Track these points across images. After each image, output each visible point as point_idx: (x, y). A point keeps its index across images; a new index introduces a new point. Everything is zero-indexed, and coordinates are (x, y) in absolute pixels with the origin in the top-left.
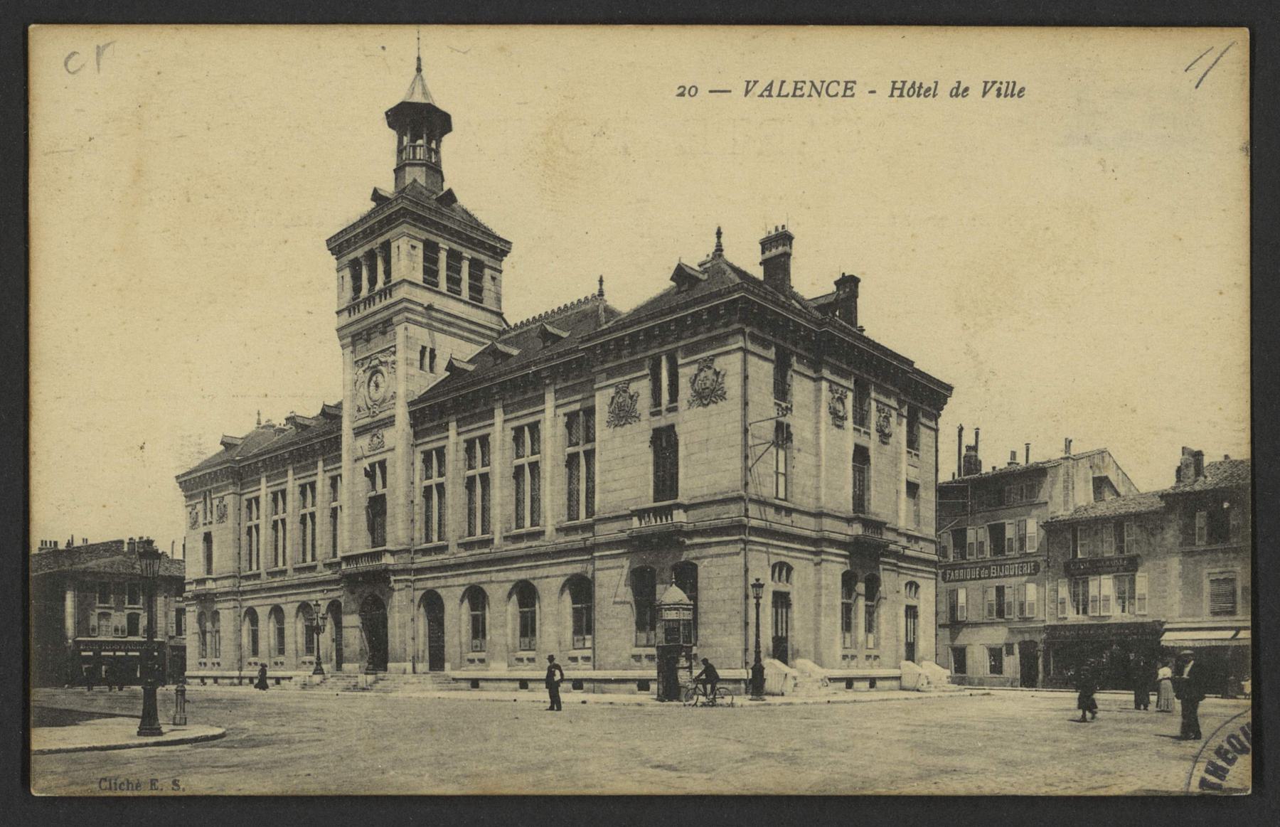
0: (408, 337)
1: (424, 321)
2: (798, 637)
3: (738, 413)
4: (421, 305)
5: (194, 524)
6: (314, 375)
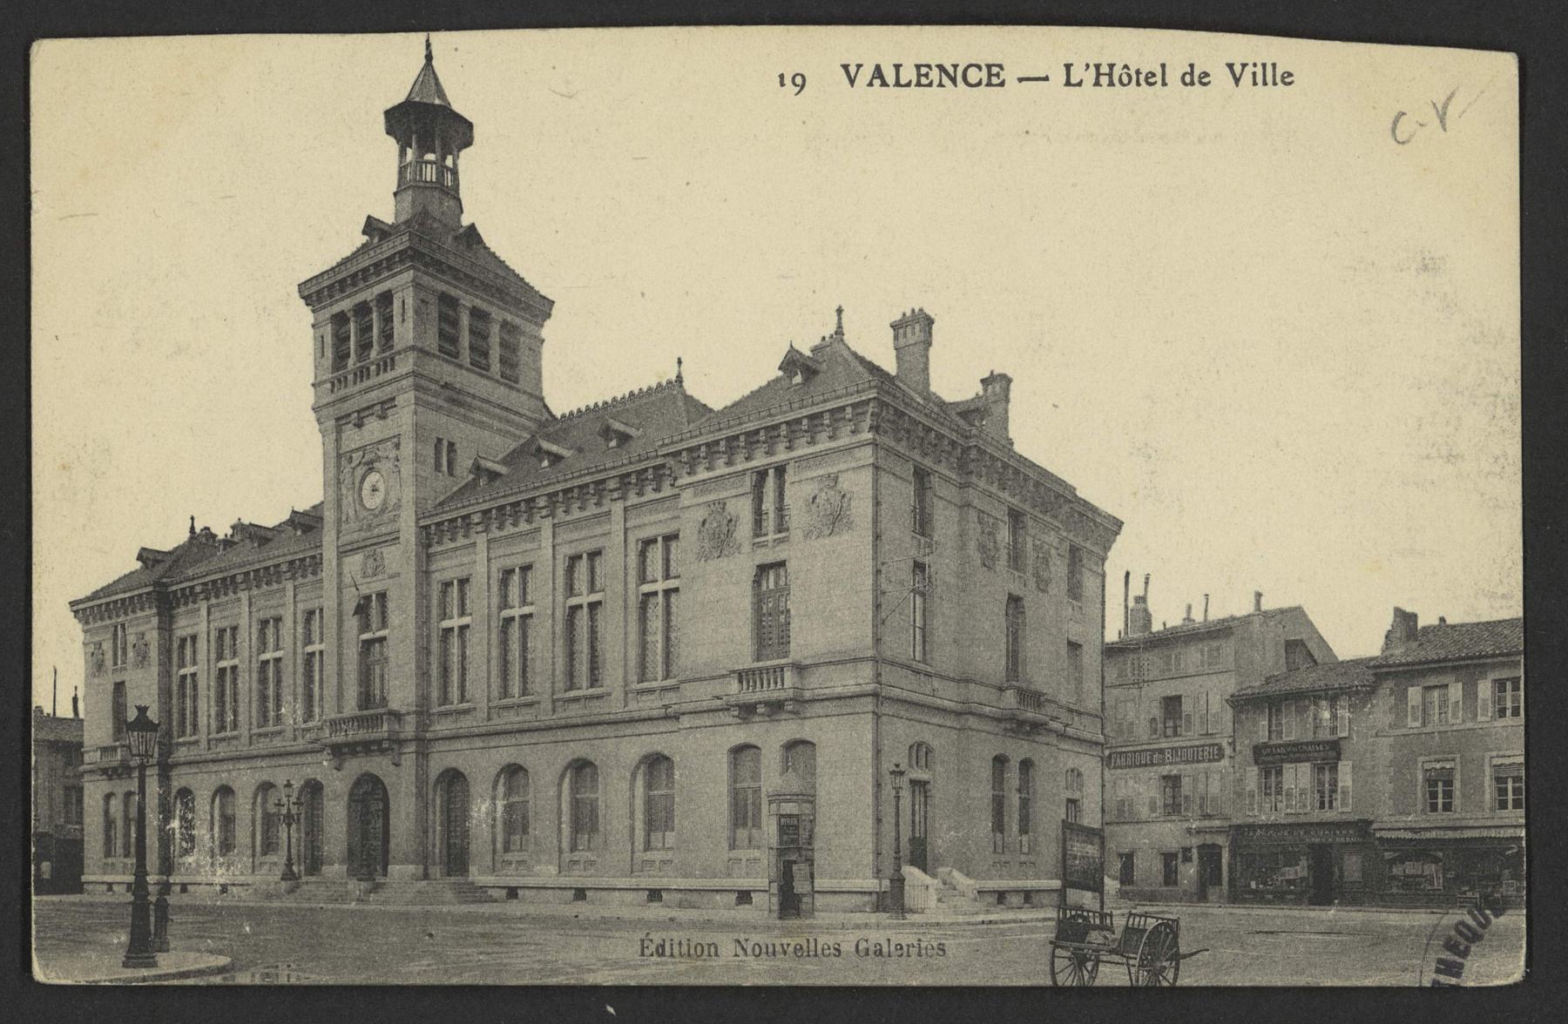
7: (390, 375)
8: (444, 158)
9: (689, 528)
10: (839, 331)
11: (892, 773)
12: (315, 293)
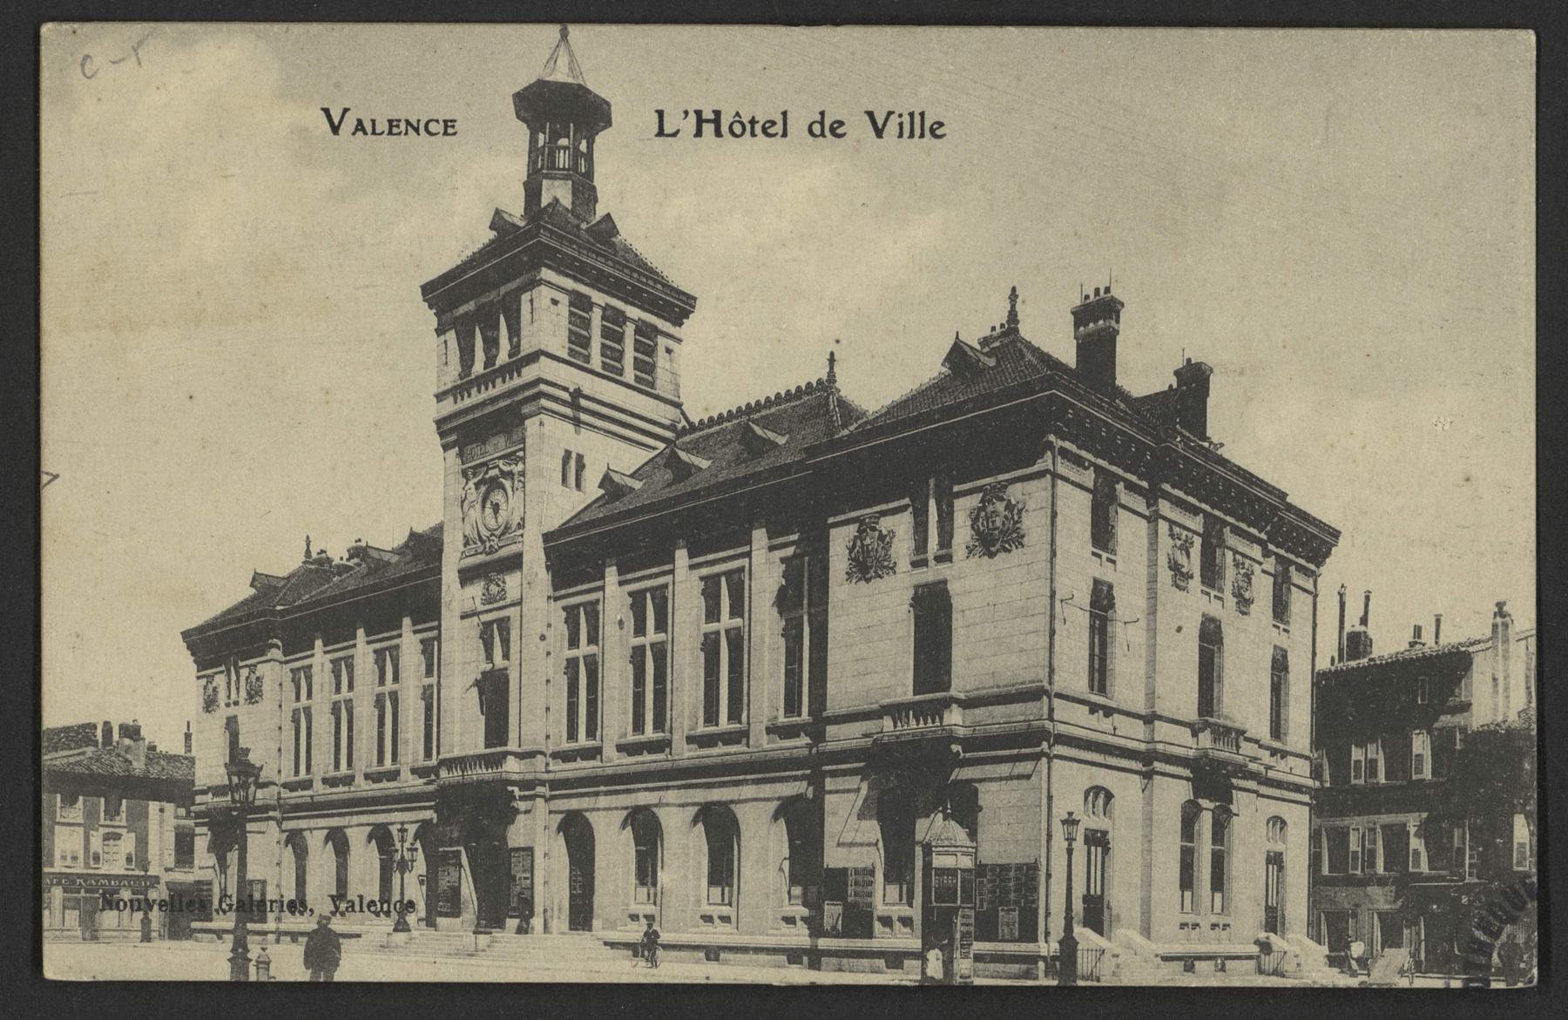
0: (548, 435)
1: (568, 411)
2: (1122, 898)
3: (1042, 567)
4: (565, 389)
5: (210, 704)
6: (398, 490)
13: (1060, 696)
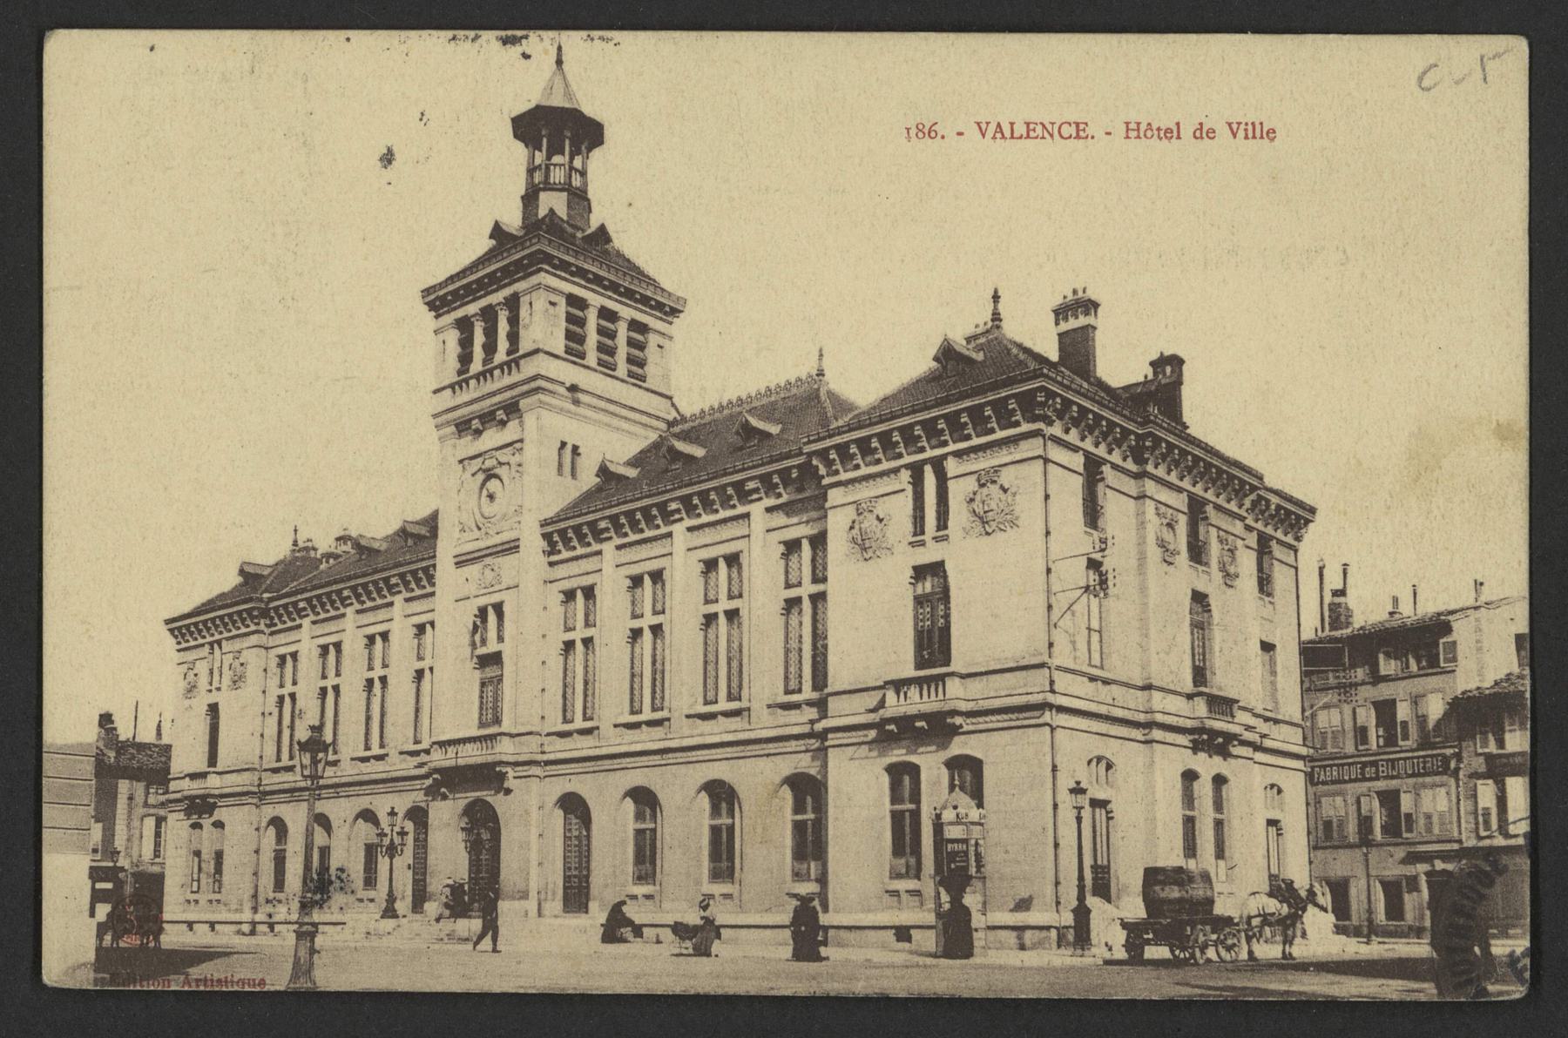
0: (543, 426)
7: (516, 377)
8: (572, 159)
9: (838, 523)
10: (996, 317)
11: (1072, 791)
12: (439, 300)
13: (1058, 668)
